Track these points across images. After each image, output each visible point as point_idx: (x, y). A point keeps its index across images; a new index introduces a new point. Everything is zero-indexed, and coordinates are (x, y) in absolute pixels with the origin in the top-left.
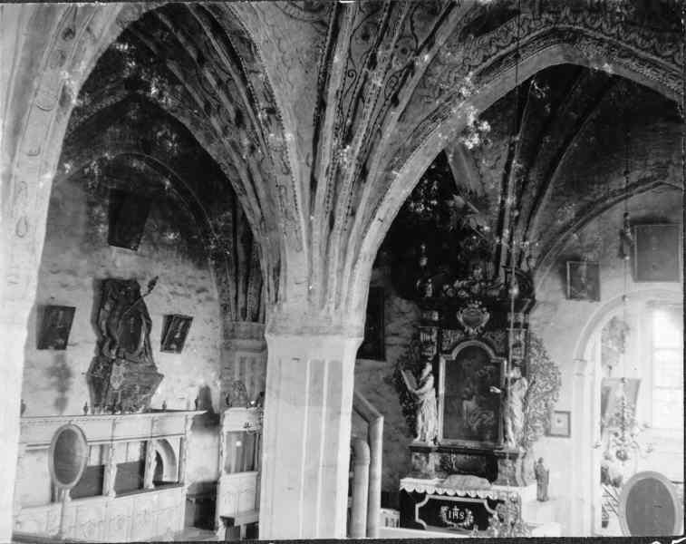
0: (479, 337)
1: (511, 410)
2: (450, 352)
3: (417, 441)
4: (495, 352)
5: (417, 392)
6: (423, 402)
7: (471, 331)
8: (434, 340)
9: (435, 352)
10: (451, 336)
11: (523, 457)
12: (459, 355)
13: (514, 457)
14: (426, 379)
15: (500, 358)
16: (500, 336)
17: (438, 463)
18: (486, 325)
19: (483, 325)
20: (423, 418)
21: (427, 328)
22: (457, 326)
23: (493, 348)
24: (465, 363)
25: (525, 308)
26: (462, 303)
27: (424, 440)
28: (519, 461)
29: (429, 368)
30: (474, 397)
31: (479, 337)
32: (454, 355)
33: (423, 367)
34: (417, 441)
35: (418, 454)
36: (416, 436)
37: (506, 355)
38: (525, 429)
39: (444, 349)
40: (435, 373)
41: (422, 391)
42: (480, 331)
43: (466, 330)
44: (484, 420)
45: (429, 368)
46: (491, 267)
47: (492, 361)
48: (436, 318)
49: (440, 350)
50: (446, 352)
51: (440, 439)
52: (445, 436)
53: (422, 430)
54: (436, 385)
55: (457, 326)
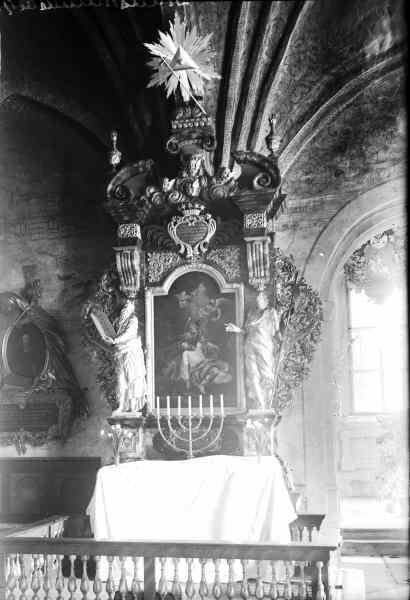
1: (257, 353)
2: (161, 283)
3: (118, 413)
6: (125, 355)
7: (190, 254)
10: (159, 261)
12: (174, 287)
15: (235, 285)
16: (232, 254)
17: (150, 442)
18: (210, 240)
19: (207, 240)
22: (168, 246)
23: (223, 272)
25: (270, 207)
26: (176, 211)
27: (130, 411)
30: (199, 345)
34: (118, 413)
37: (244, 278)
39: (151, 281)
40: (141, 314)
43: (182, 251)
47: (223, 291)
48: (139, 235)
49: (147, 283)
50: (155, 285)
53: (127, 394)
54: (142, 330)
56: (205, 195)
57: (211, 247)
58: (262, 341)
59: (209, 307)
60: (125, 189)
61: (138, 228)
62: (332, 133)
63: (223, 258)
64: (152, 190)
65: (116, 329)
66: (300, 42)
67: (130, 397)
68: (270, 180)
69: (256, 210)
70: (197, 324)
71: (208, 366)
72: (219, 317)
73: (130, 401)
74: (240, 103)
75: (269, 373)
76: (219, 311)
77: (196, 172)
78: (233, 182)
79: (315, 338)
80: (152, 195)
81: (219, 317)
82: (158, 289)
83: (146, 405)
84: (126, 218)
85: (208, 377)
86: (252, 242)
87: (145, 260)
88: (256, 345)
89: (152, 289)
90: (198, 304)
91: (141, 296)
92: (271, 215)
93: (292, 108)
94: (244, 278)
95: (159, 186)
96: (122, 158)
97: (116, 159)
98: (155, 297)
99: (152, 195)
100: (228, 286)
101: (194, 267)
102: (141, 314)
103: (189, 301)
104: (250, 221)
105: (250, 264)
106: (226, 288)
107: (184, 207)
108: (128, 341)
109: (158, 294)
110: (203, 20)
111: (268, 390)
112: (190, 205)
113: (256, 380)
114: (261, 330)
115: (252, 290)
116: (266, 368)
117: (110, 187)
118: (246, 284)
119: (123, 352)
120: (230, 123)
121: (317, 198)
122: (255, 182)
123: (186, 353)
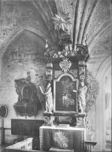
0: (68, 72)
1: (81, 98)
2: (57, 78)
4: (74, 77)
5: (45, 94)
6: (48, 97)
7: (65, 70)
8: (51, 74)
9: (52, 79)
10: (57, 73)
11: (86, 116)
13: (83, 116)
14: (49, 88)
15: (76, 79)
16: (76, 71)
17: (54, 119)
18: (70, 67)
19: (69, 67)
20: (48, 103)
21: (48, 70)
22: (59, 69)
23: (73, 76)
24: (63, 82)
26: (61, 60)
28: (85, 118)
29: (49, 85)
30: (67, 95)
31: (68, 72)
32: (59, 80)
33: (47, 84)
34: (46, 112)
35: (46, 117)
36: (46, 110)
37: (78, 78)
38: (87, 106)
39: (55, 78)
40: (52, 86)
41: (47, 93)
42: (68, 70)
43: (63, 70)
44: (71, 103)
45: (49, 85)
46: (71, 45)
47: (73, 81)
50: (56, 79)
51: (55, 111)
52: (56, 110)
54: (52, 91)
55: (59, 69)
56: (69, 56)
57: (70, 69)
58: (82, 95)
59: (70, 85)
60: (48, 53)
61: (52, 64)
62: (105, 37)
63: (73, 72)
64: (55, 55)
65: (46, 90)
66: (96, 14)
67: (49, 108)
68: (85, 51)
69: (82, 60)
70: (66, 89)
71: (69, 100)
72: (72, 88)
73: (49, 109)
74: (79, 31)
75: (84, 104)
76: (72, 86)
77: (67, 49)
78: (76, 52)
79: (97, 94)
80: (55, 55)
81: (72, 88)
82: (56, 80)
83: (53, 110)
84: (48, 62)
85: (69, 103)
86: (80, 68)
87: (54, 73)
88: (81, 96)
89: (55, 80)
90: (67, 85)
91: (52, 81)
92: (86, 61)
93: (93, 31)
94: (78, 78)
95: (57, 53)
96: (48, 46)
97: (47, 46)
98: (56, 82)
99: (55, 55)
100: (75, 79)
101: (66, 74)
102: (52, 86)
103: (64, 83)
104: (80, 63)
105: (80, 74)
106: (74, 80)
107: (63, 59)
108: (48, 93)
109: (56, 81)
110: (68, 10)
111: (84, 107)
112: (65, 59)
113: (80, 105)
114: (82, 92)
115: (80, 81)
116: (83, 102)
117: (45, 53)
118: (79, 79)
119: (47, 96)
120: (76, 36)
121: (100, 55)
122: (82, 52)
123: (63, 97)
